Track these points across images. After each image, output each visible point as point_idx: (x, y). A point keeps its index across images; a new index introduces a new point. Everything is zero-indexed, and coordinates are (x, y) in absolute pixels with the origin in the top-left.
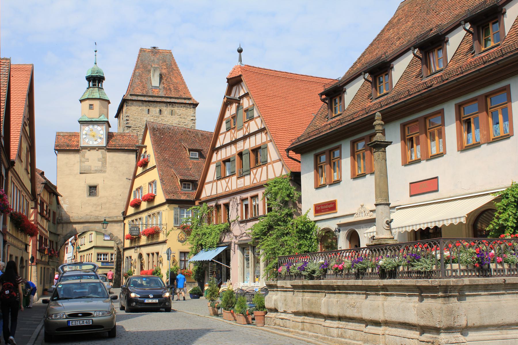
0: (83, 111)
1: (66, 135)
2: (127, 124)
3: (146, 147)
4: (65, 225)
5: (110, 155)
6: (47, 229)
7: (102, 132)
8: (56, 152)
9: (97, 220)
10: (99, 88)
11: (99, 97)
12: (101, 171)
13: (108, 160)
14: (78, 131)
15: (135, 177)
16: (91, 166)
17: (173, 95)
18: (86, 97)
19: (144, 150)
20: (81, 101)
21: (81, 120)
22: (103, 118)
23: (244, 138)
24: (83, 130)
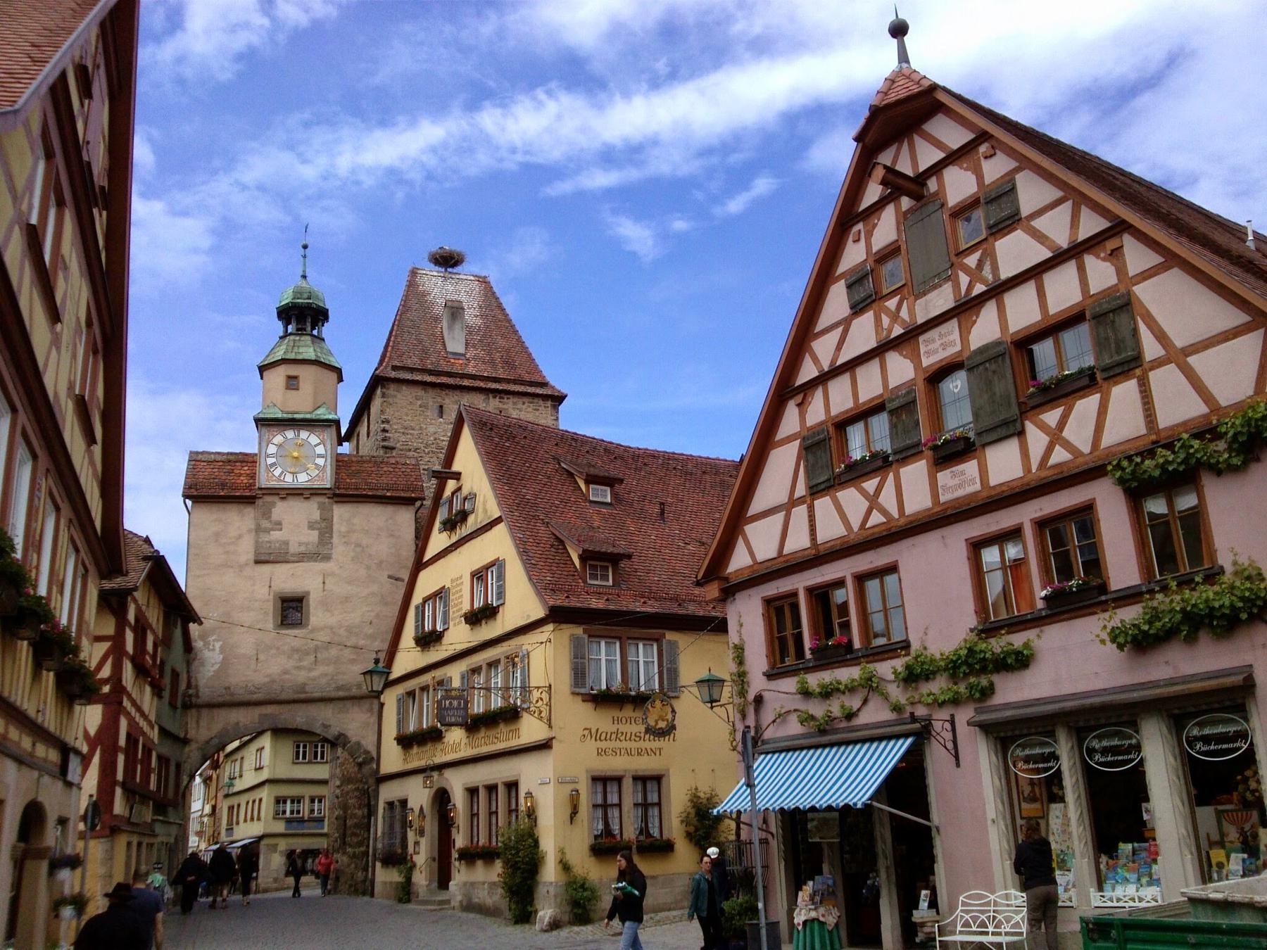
0: (272, 395)
1: (219, 458)
2: (384, 440)
3: (457, 476)
4: (205, 712)
5: (341, 513)
6: (153, 718)
7: (320, 450)
8: (189, 502)
9: (302, 696)
10: (312, 335)
11: (313, 358)
12: (319, 554)
13: (338, 526)
14: (253, 449)
15: (420, 565)
16: (287, 543)
17: (501, 373)
18: (279, 355)
19: (451, 485)
20: (262, 369)
21: (261, 416)
22: (323, 413)
23: (966, 309)
24: (269, 442)
